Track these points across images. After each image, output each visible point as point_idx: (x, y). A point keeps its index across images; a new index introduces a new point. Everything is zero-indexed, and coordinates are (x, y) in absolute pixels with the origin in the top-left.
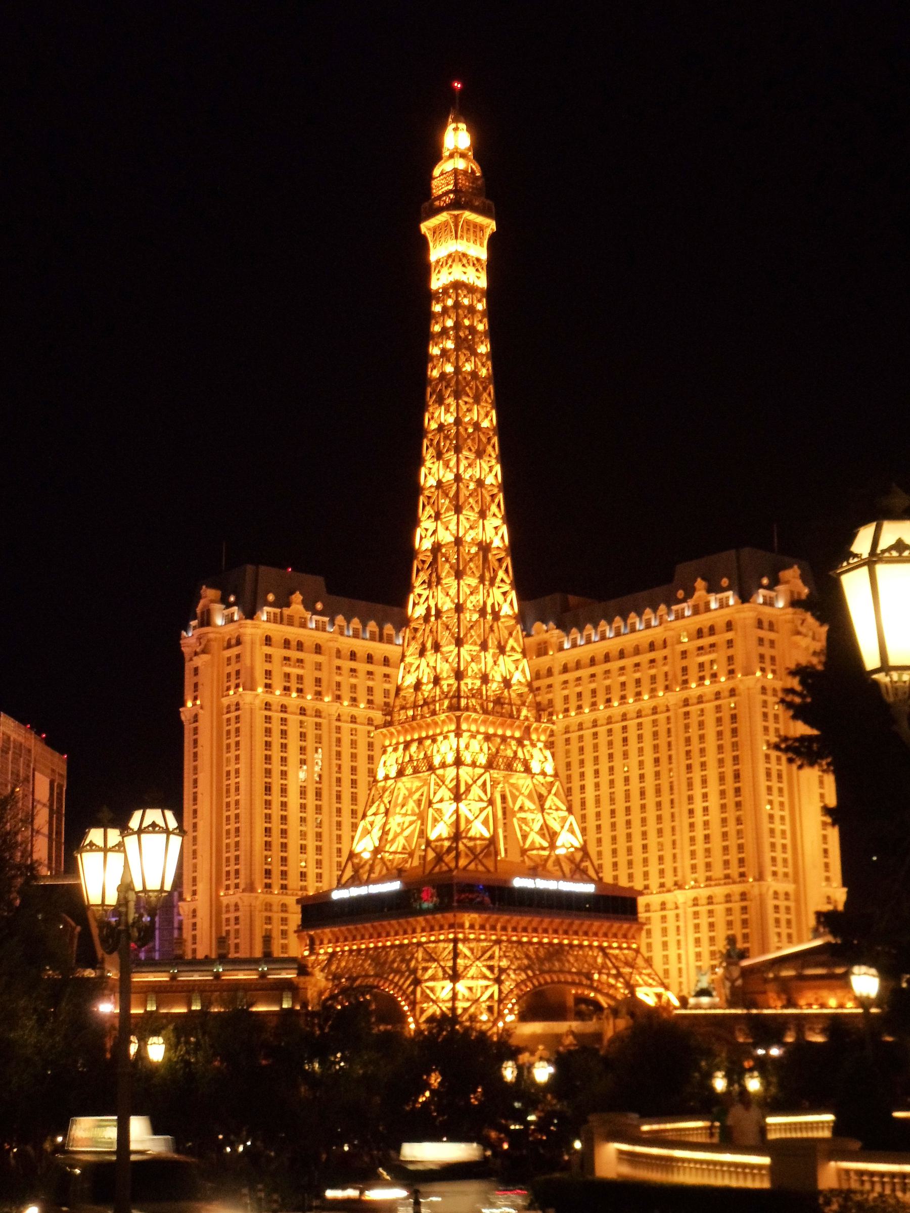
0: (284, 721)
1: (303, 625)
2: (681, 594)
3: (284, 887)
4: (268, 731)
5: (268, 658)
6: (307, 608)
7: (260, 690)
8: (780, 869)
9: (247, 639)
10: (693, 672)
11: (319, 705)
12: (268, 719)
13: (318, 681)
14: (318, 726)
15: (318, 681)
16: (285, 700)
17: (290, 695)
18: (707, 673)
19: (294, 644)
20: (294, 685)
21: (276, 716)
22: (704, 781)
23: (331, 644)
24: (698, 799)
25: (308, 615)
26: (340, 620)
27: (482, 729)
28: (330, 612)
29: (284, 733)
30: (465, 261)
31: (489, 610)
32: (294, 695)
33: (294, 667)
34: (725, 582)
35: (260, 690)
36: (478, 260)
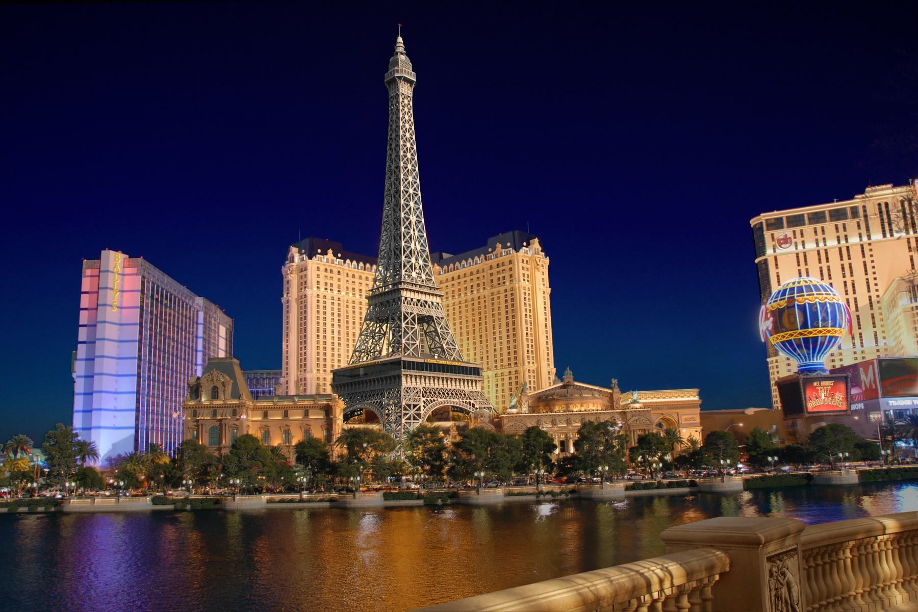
0: (325, 302)
1: (333, 262)
2: (490, 250)
3: (325, 371)
4: (318, 306)
5: (318, 276)
8: (531, 361)
9: (309, 268)
10: (495, 282)
11: (339, 296)
12: (318, 301)
14: (339, 304)
18: (501, 282)
20: (329, 287)
21: (322, 300)
22: (500, 327)
24: (497, 333)
26: (348, 261)
28: (344, 258)
29: (325, 307)
34: (509, 244)
35: (315, 289)
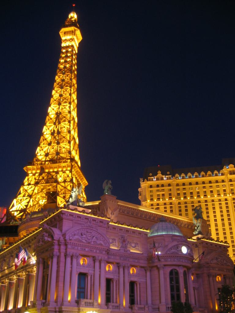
1: (162, 179)
6: (163, 174)
7: (149, 201)
11: (171, 201)
13: (170, 194)
14: (171, 207)
15: (170, 194)
16: (158, 202)
17: (160, 200)
19: (160, 185)
20: (161, 197)
23: (173, 182)
25: (164, 176)
26: (177, 175)
30: (65, 41)
31: (56, 132)
32: (161, 200)
33: (161, 192)
35: (149, 201)
36: (71, 39)
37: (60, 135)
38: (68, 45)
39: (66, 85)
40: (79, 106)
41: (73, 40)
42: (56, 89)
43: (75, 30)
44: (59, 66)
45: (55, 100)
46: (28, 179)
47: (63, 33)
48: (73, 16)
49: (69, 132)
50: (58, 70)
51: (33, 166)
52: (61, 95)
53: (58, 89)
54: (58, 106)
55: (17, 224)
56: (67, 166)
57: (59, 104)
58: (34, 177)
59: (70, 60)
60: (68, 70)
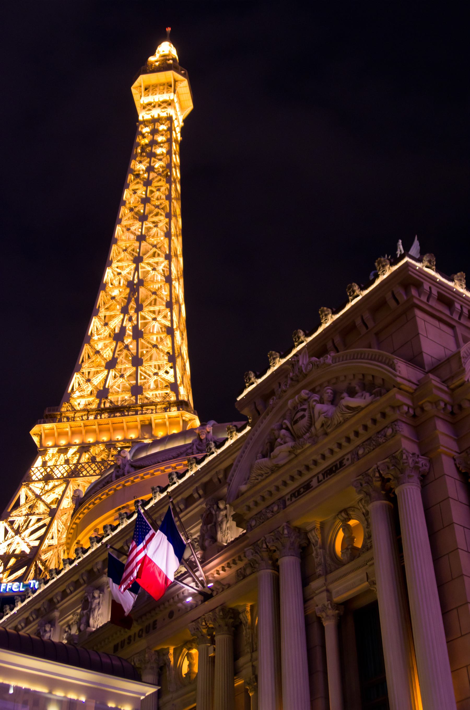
27: (77, 441)
31: (129, 332)
36: (164, 102)
37: (141, 341)
38: (156, 116)
39: (155, 213)
40: (188, 274)
41: (170, 104)
42: (124, 223)
43: (175, 81)
44: (132, 166)
45: (125, 250)
46: (44, 464)
47: (143, 89)
48: (166, 49)
49: (170, 331)
50: (131, 177)
51: (60, 425)
52: (141, 238)
53: (130, 222)
54: (134, 265)
55: (11, 589)
56: (167, 423)
57: (138, 260)
58: (62, 458)
59: (164, 150)
60: (159, 174)
